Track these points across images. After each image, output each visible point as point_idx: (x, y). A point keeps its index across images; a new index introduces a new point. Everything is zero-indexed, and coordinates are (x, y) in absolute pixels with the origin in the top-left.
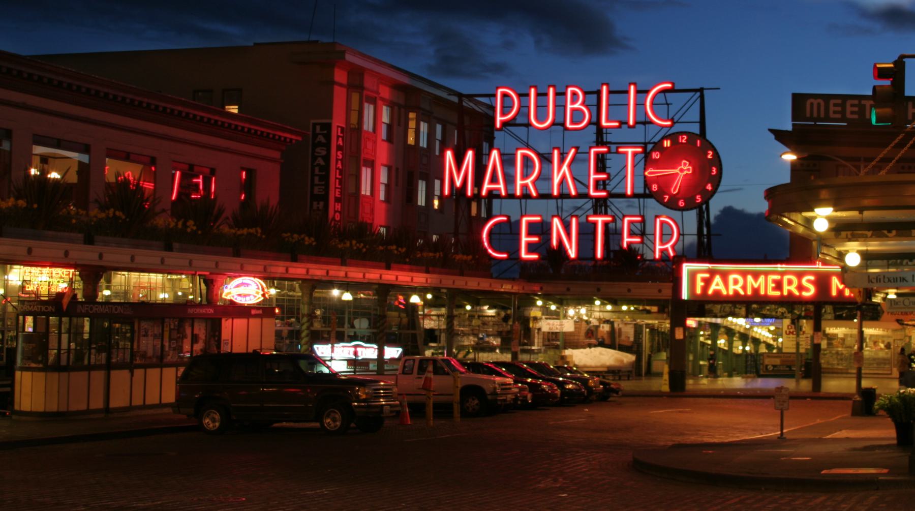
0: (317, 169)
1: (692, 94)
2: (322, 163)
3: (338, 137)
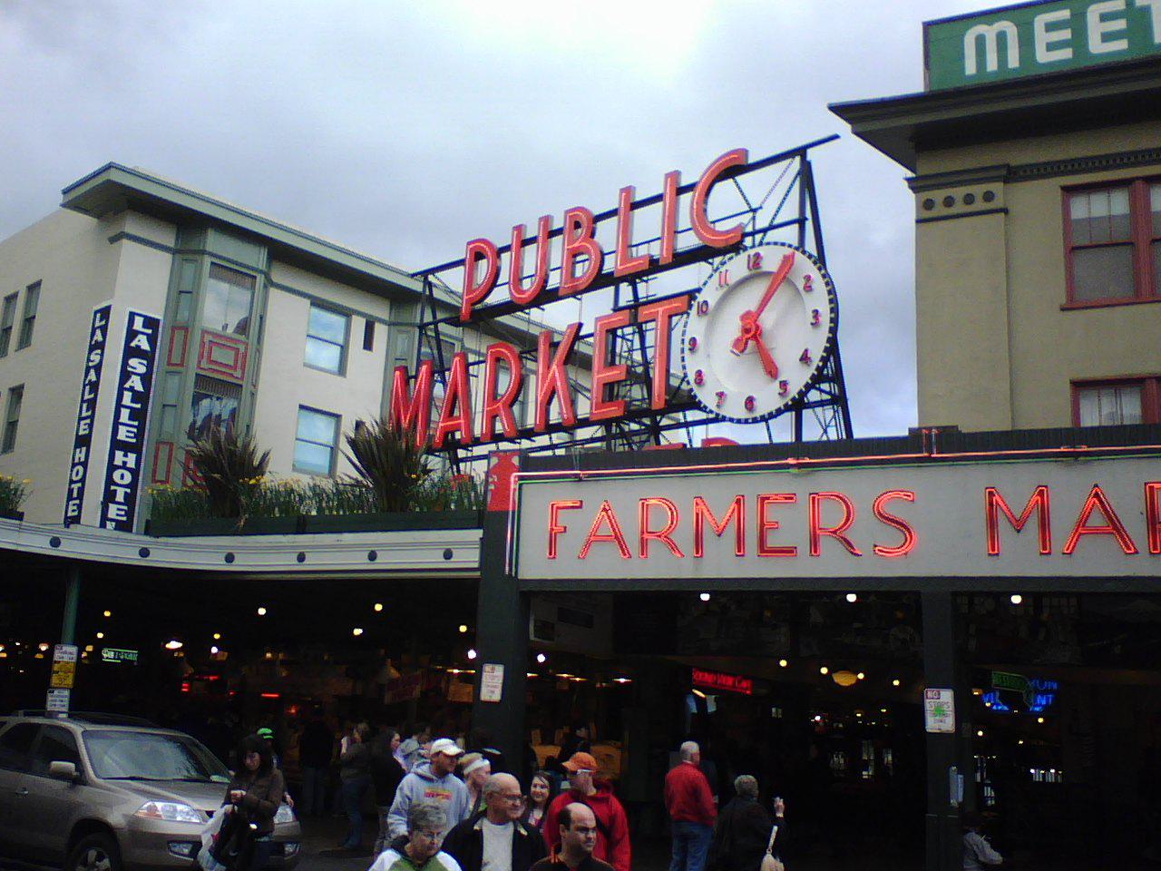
1: (788, 161)
3: (132, 334)
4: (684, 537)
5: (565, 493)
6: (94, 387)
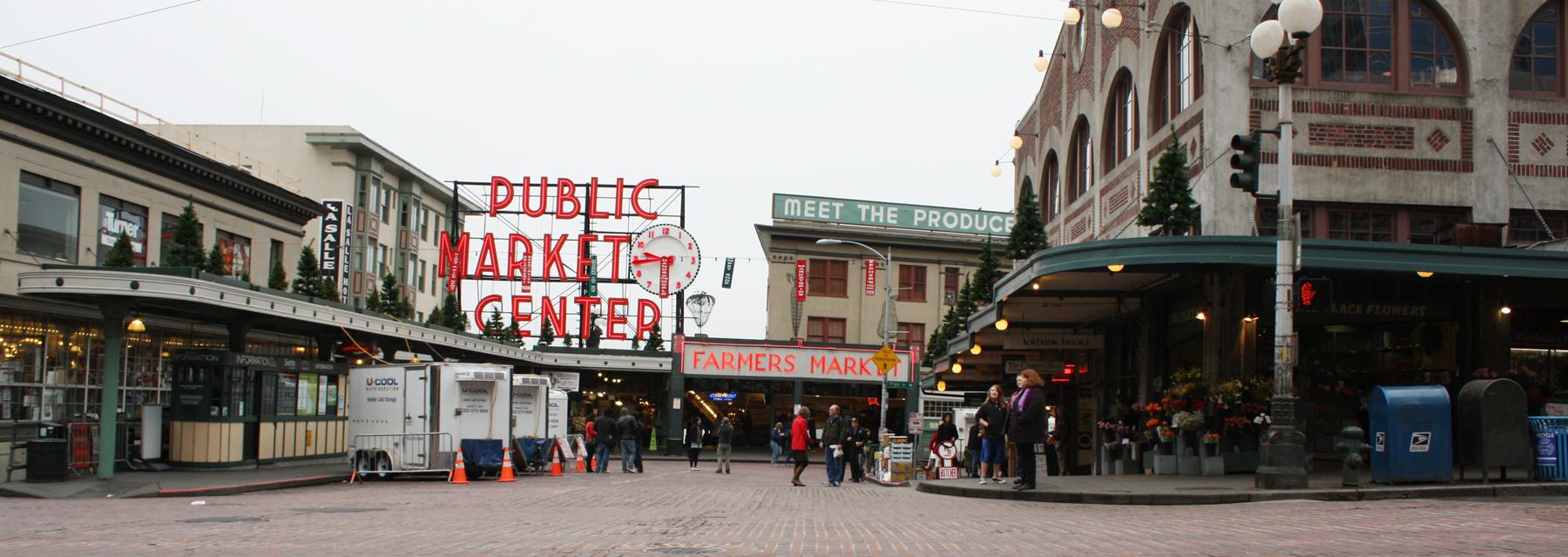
0: (327, 247)
2: (333, 239)
4: (735, 363)
5: (699, 349)
6: (335, 245)
